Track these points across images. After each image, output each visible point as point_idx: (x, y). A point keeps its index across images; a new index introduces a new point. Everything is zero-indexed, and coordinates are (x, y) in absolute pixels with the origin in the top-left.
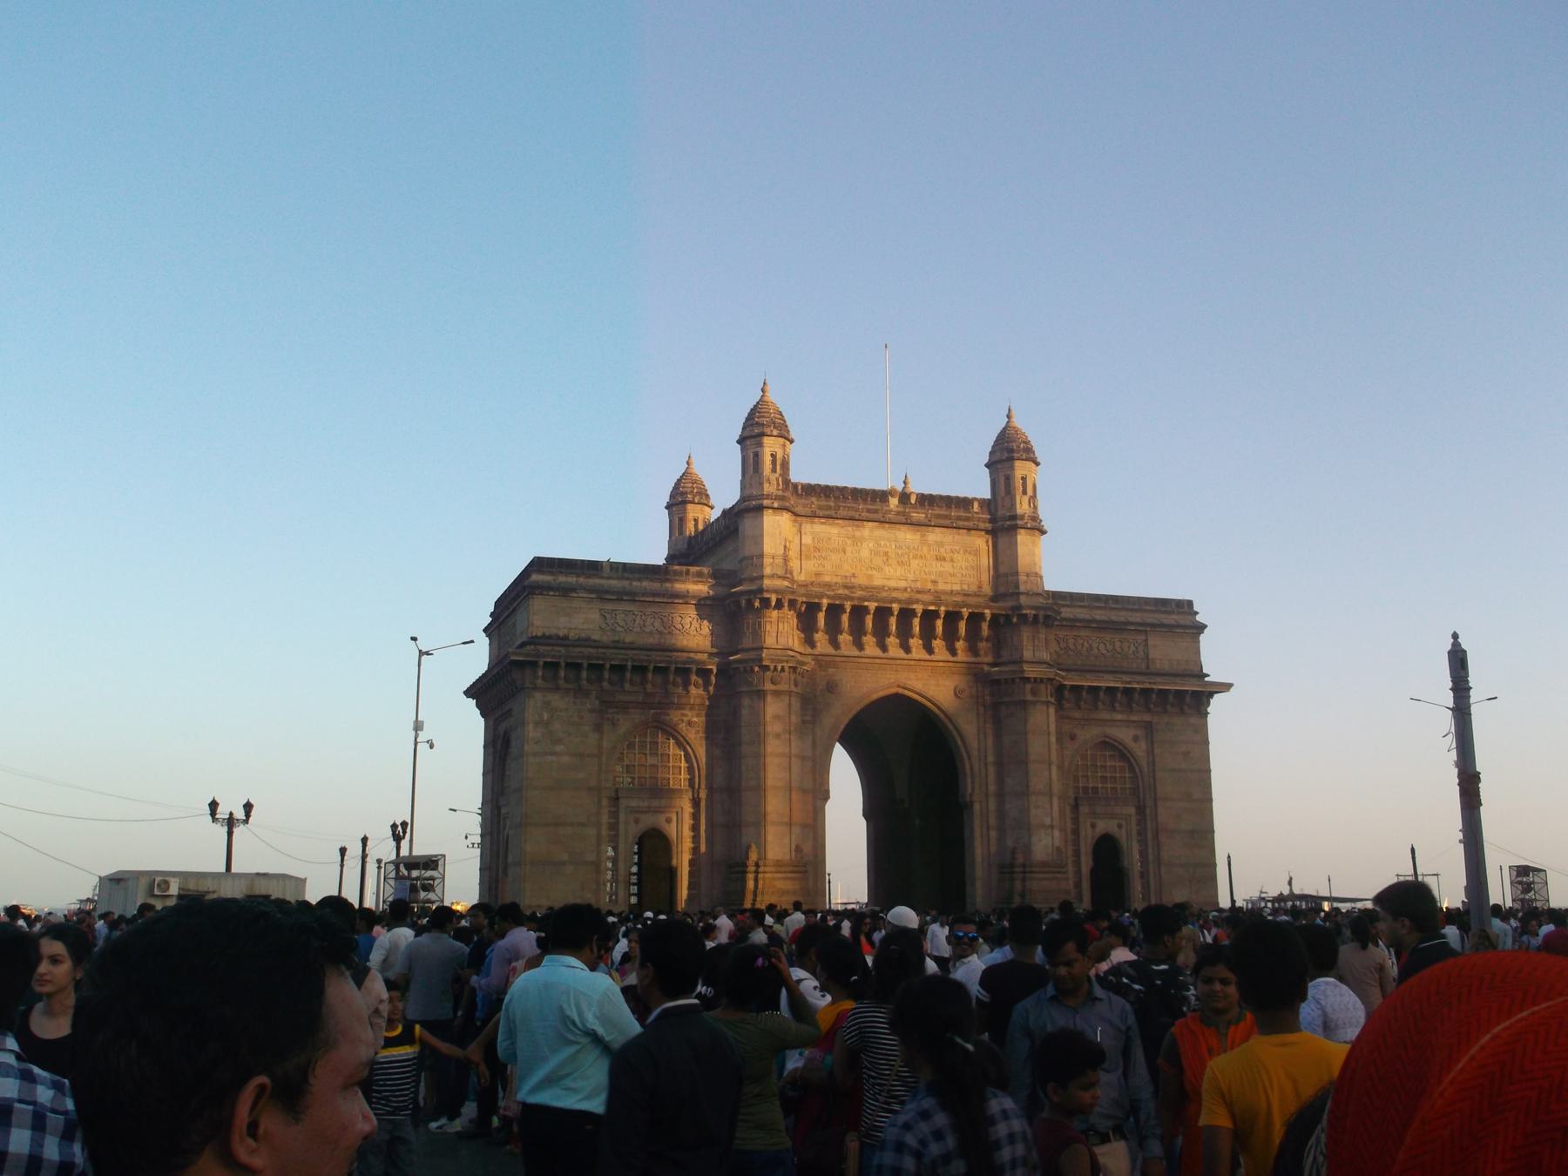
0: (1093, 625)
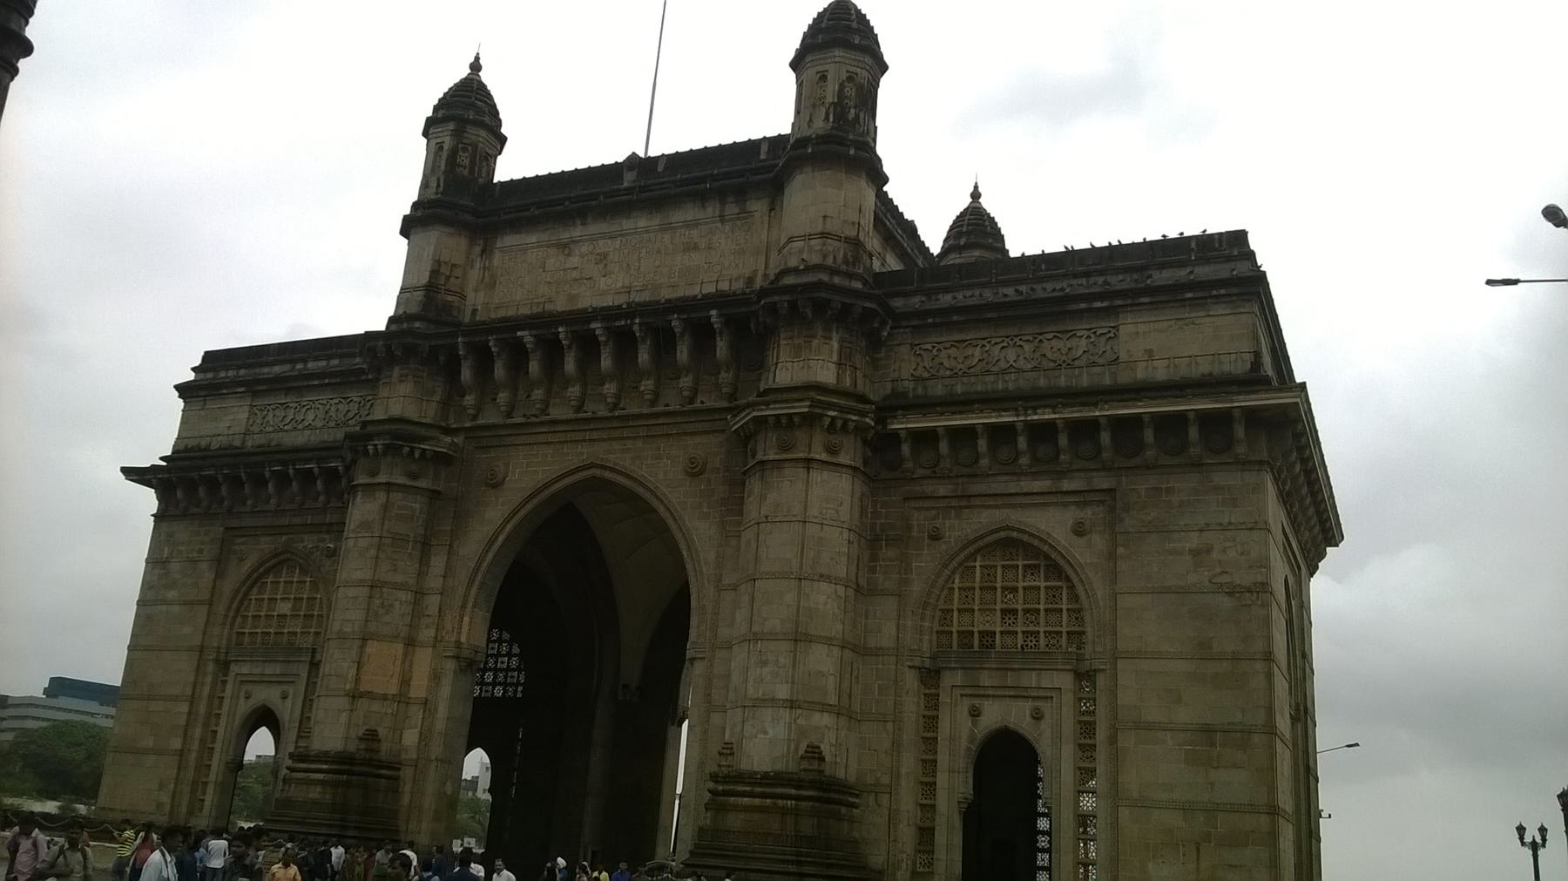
0: (990, 315)
